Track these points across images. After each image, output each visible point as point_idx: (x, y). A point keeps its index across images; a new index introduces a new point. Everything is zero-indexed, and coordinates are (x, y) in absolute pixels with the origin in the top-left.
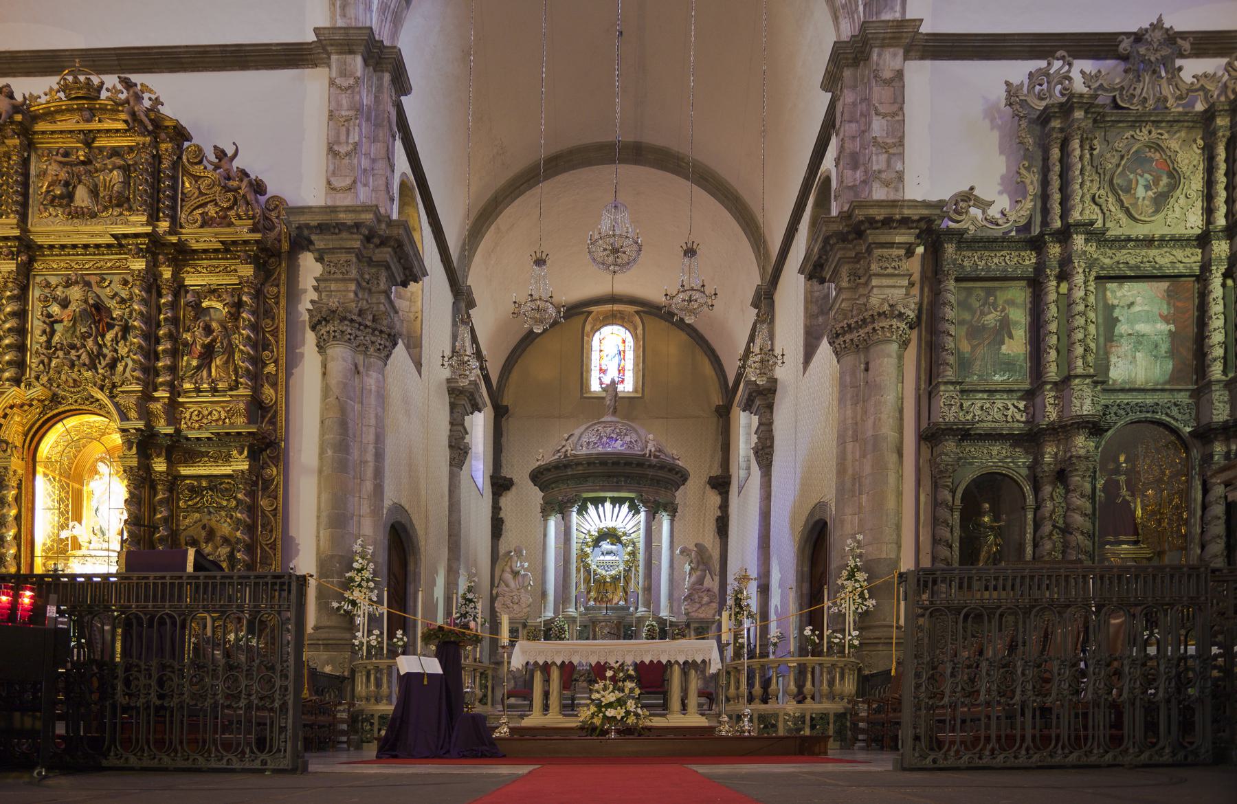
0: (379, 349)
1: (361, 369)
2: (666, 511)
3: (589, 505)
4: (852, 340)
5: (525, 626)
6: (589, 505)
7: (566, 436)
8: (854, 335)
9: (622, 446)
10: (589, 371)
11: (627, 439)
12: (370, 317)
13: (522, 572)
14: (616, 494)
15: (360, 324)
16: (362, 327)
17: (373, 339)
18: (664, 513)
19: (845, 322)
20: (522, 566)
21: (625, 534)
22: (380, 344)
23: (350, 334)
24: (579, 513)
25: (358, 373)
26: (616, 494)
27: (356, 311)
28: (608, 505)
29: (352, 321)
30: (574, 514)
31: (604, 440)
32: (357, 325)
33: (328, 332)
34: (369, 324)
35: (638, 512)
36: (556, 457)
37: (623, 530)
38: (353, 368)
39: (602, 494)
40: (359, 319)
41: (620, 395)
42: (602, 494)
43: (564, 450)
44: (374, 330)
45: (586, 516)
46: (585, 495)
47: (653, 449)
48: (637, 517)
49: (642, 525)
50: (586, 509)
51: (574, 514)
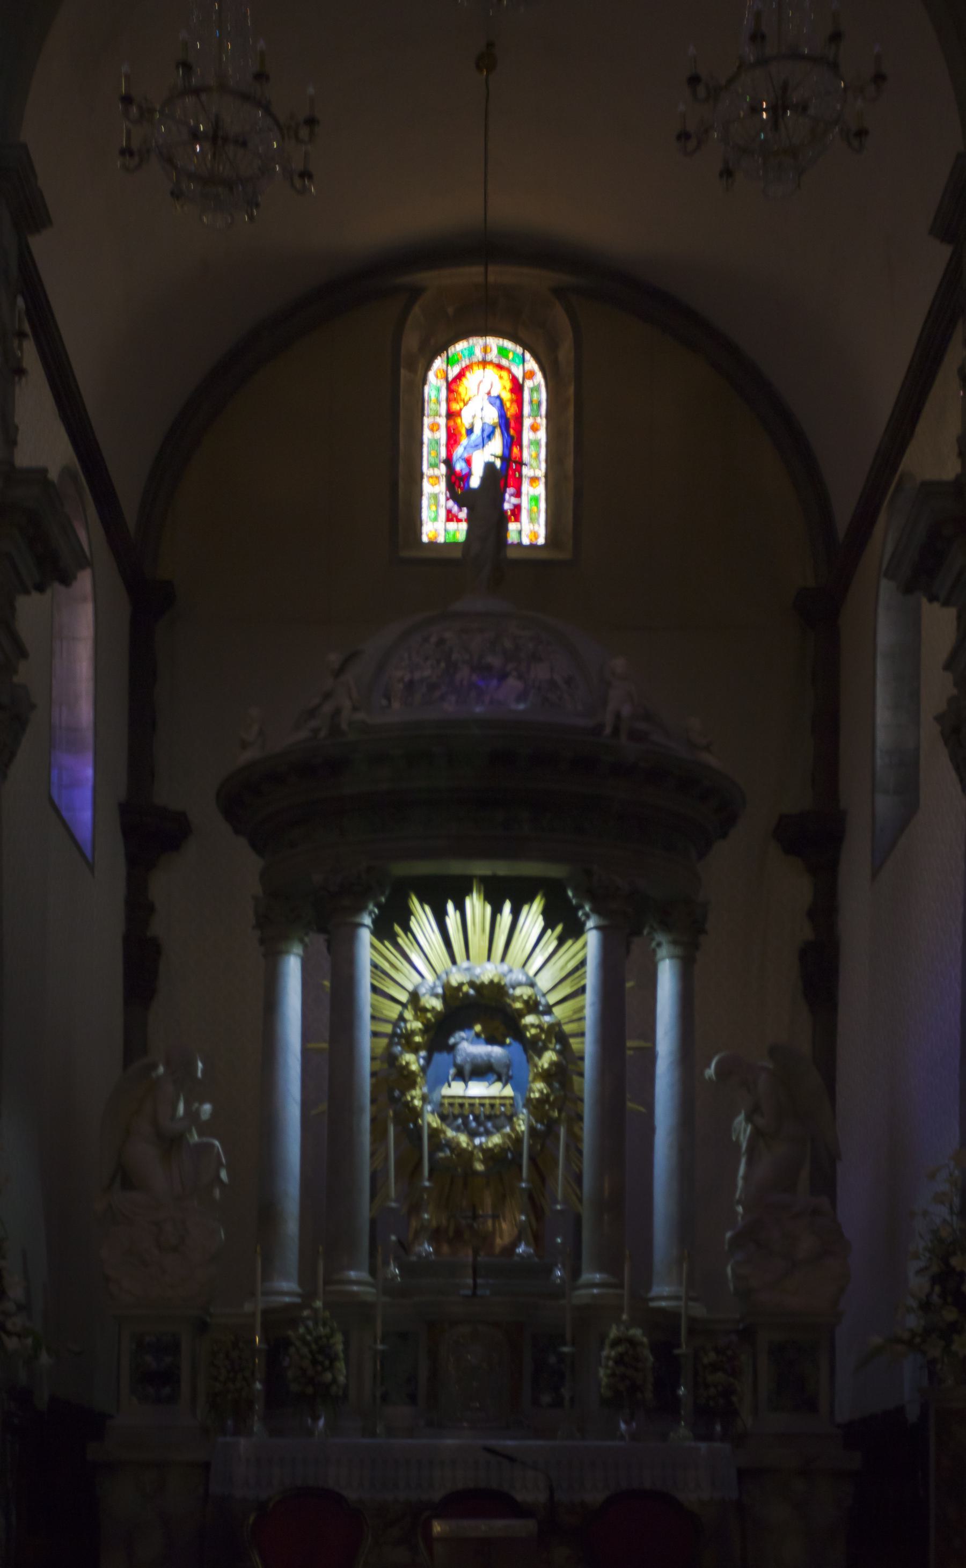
2: (666, 926)
3: (415, 904)
5: (202, 1327)
6: (415, 904)
7: (334, 658)
9: (521, 697)
10: (416, 477)
11: (540, 672)
13: (195, 1138)
14: (502, 868)
18: (660, 937)
20: (193, 1116)
21: (532, 1006)
24: (383, 932)
26: (502, 868)
28: (476, 905)
30: (366, 936)
31: (464, 673)
35: (573, 931)
36: (303, 734)
37: (524, 992)
39: (457, 867)
41: (511, 554)
42: (457, 867)
43: (328, 708)
45: (402, 940)
46: (402, 869)
47: (626, 710)
48: (571, 949)
49: (590, 977)
50: (404, 920)
51: (366, 936)
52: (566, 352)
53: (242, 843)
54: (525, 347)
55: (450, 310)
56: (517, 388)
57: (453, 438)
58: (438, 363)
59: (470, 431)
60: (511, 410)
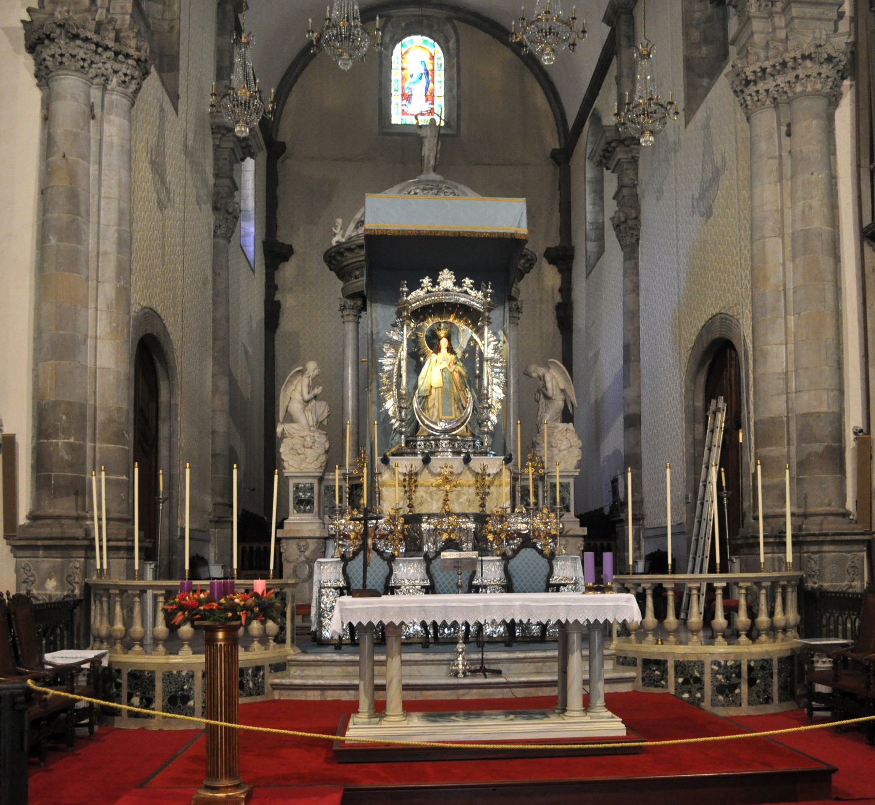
0: (124, 82)
1: (97, 111)
4: (767, 91)
8: (770, 84)
12: (112, 35)
15: (98, 45)
16: (100, 50)
17: (117, 66)
19: (759, 64)
22: (125, 75)
23: (84, 60)
25: (93, 117)
27: (92, 26)
29: (86, 40)
32: (93, 47)
33: (53, 56)
34: (111, 44)
38: (88, 110)
40: (95, 38)
44: (117, 54)
52: (452, 44)
53: (333, 274)
54: (435, 40)
55: (403, 25)
56: (432, 58)
57: (403, 79)
58: (398, 46)
59: (412, 76)
60: (429, 67)
